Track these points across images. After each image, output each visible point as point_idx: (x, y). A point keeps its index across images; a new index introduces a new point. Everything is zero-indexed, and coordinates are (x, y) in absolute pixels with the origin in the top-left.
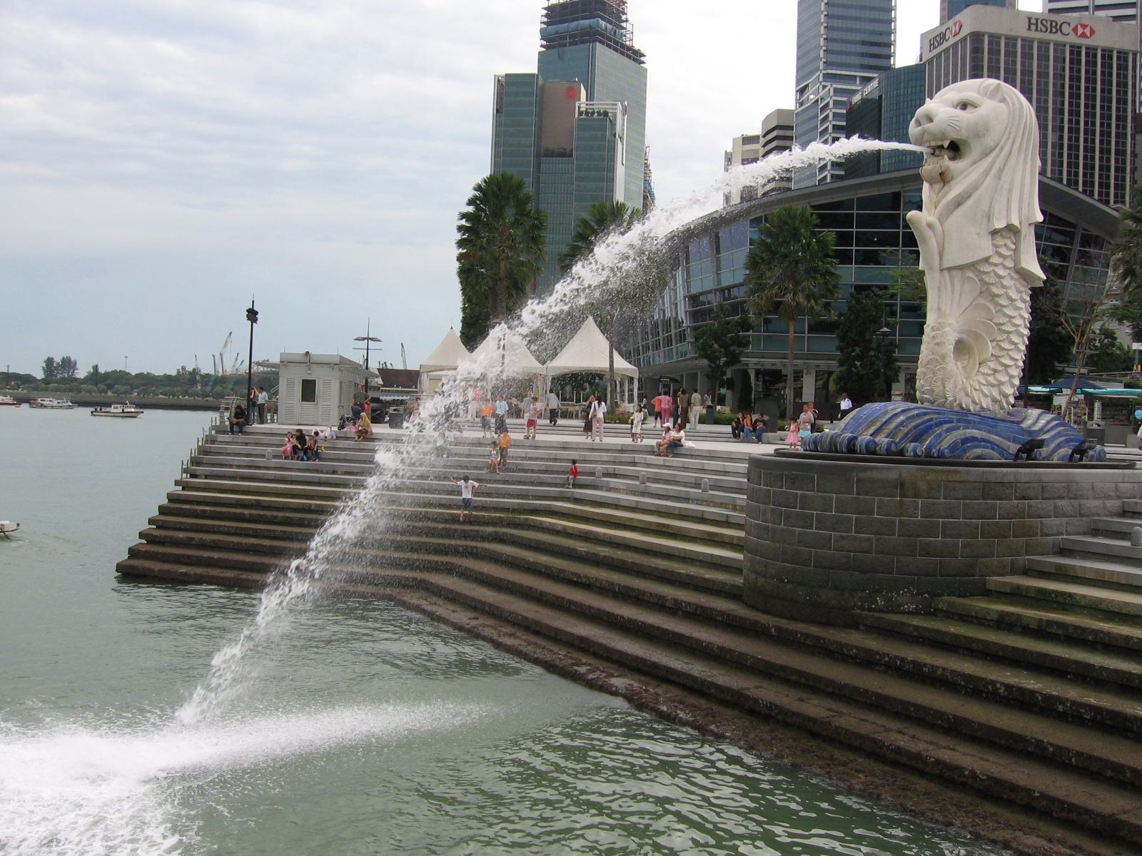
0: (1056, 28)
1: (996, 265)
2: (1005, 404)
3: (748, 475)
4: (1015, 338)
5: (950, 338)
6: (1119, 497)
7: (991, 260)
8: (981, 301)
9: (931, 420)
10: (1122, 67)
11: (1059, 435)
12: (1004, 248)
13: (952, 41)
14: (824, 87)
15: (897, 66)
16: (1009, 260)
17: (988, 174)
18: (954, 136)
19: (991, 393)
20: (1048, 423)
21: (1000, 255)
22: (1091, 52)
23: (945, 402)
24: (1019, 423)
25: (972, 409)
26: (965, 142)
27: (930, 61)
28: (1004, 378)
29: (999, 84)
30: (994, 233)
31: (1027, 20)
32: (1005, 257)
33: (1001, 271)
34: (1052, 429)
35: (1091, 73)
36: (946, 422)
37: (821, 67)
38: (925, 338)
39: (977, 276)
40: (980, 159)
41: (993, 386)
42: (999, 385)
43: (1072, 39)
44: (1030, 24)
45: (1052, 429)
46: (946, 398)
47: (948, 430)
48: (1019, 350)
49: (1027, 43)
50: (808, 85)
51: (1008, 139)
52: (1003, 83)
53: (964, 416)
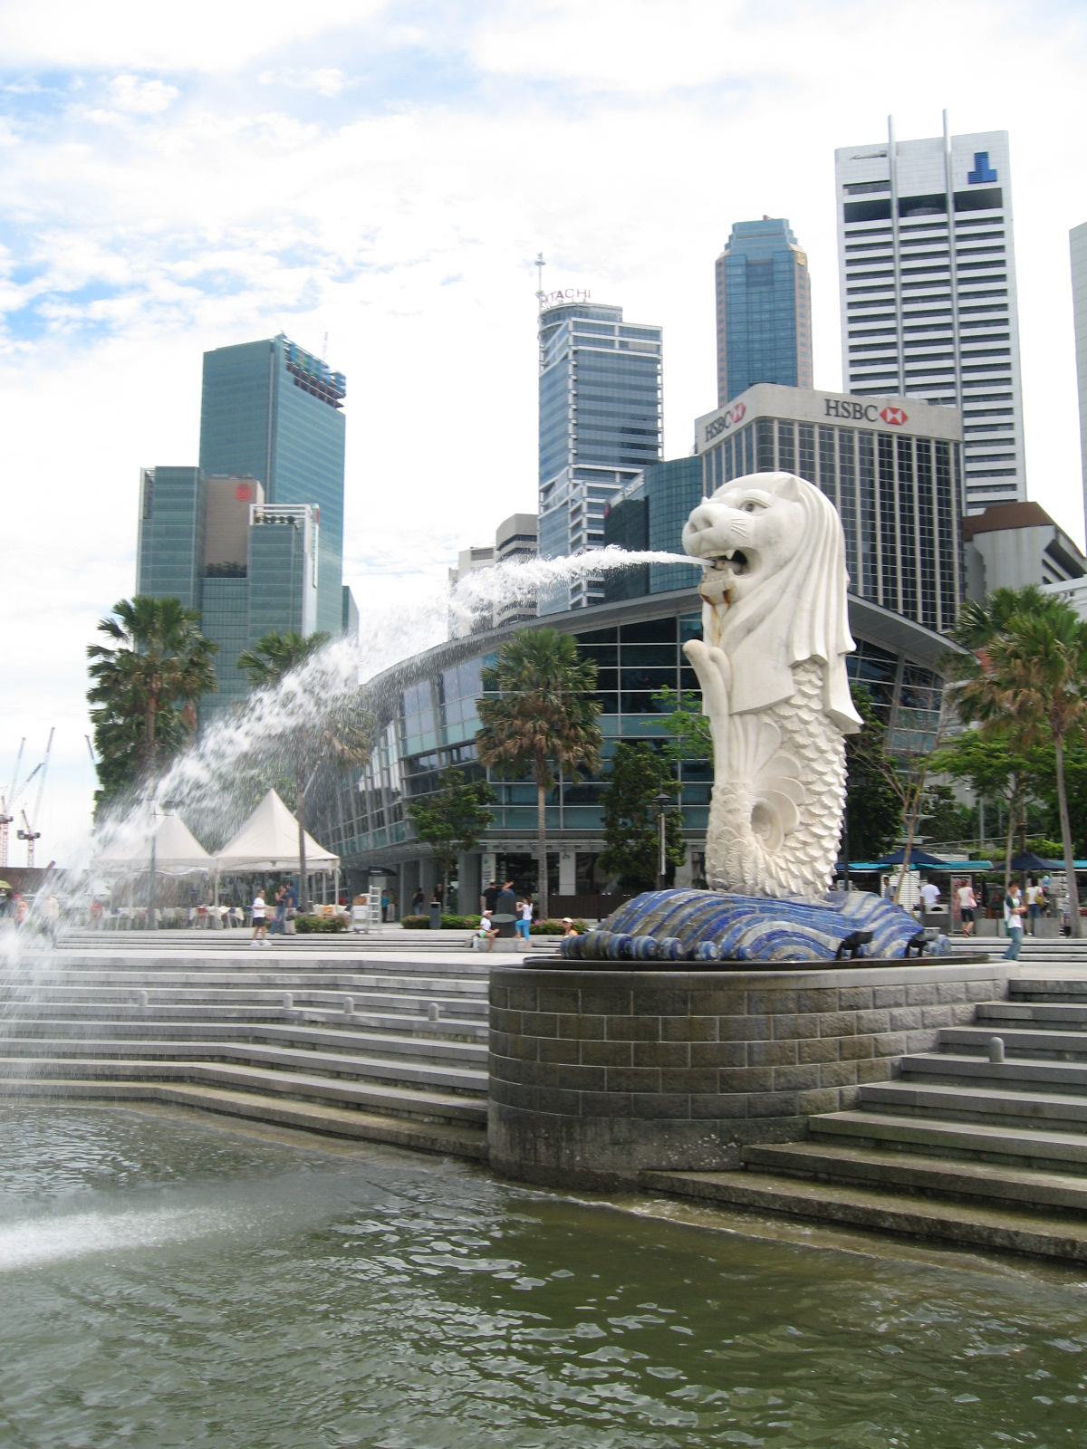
0: (861, 413)
1: (799, 707)
2: (820, 886)
3: (491, 996)
4: (827, 800)
5: (747, 802)
6: (970, 1001)
7: (793, 701)
8: (784, 753)
9: (725, 911)
10: (943, 461)
11: (890, 923)
12: (808, 685)
13: (733, 428)
14: (575, 485)
15: (667, 458)
16: (816, 699)
17: (784, 592)
18: (739, 543)
19: (800, 870)
20: (876, 908)
21: (805, 695)
22: (904, 442)
23: (743, 887)
24: (838, 910)
25: (778, 894)
26: (753, 552)
27: (708, 454)
28: (816, 852)
29: (792, 479)
30: (796, 666)
31: (824, 403)
32: (809, 697)
33: (806, 715)
34: (882, 915)
36: (746, 913)
37: (571, 461)
38: (713, 804)
39: (776, 722)
40: (774, 573)
41: (802, 862)
42: (811, 862)
43: (881, 426)
44: (829, 407)
45: (882, 915)
46: (744, 881)
47: (748, 924)
48: (833, 816)
49: (826, 430)
50: (553, 484)
51: (807, 547)
52: (798, 479)
53: (768, 904)
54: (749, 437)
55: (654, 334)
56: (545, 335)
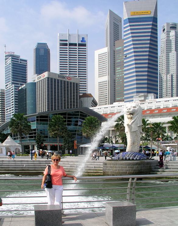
0: (64, 77)
10: (77, 86)
13: (42, 79)
14: (12, 85)
22: (71, 83)
27: (38, 82)
35: (71, 87)
43: (67, 80)
49: (58, 80)
54: (45, 80)
55: (26, 61)
56: (6, 59)
